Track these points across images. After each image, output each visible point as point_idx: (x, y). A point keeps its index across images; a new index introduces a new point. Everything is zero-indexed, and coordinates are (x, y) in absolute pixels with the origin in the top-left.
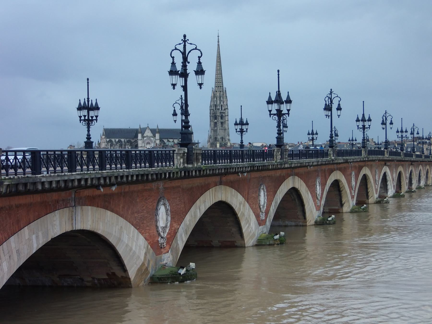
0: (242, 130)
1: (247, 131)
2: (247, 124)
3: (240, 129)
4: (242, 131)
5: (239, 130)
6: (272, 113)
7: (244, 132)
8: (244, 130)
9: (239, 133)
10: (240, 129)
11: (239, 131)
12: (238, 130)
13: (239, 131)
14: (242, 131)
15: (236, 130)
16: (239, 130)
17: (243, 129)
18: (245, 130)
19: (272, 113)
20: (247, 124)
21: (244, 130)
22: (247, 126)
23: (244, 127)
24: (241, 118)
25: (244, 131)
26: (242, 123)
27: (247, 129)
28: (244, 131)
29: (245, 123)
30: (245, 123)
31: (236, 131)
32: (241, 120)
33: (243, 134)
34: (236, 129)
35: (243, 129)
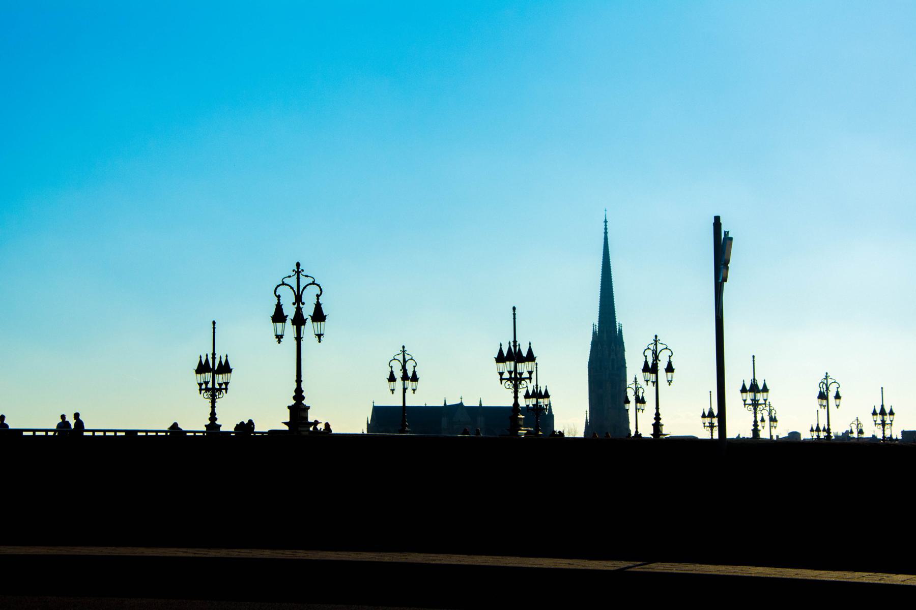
7: (523, 382)
8: (523, 376)
9: (509, 382)
10: (510, 372)
17: (521, 374)
18: (526, 375)
20: (531, 357)
21: (523, 376)
24: (515, 342)
25: (524, 379)
28: (524, 379)
29: (525, 354)
30: (525, 354)
31: (502, 379)
32: (515, 346)
35: (521, 374)
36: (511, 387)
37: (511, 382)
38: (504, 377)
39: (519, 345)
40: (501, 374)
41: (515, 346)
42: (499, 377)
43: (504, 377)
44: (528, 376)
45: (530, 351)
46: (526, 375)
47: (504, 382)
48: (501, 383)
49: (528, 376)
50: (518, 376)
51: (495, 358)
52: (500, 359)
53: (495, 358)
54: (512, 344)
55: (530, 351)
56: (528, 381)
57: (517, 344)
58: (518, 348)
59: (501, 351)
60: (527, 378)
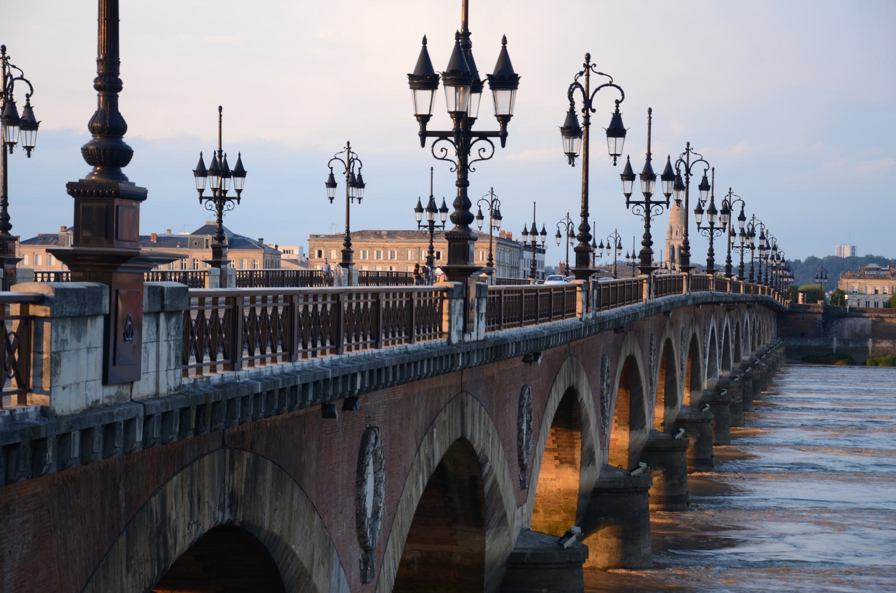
0: (220, 193)
1: (239, 199)
2: (240, 172)
3: (215, 190)
4: (220, 198)
5: (211, 194)
7: (227, 203)
8: (228, 195)
9: (212, 202)
10: (215, 190)
11: (210, 199)
12: (208, 193)
13: (210, 199)
14: (220, 198)
15: (201, 194)
16: (211, 194)
17: (225, 192)
18: (231, 193)
20: (240, 172)
21: (228, 195)
22: (239, 179)
23: (230, 185)
24: (220, 151)
25: (230, 199)
26: (220, 169)
28: (230, 199)
29: (232, 167)
30: (232, 167)
31: (201, 198)
32: (220, 156)
33: (225, 207)
34: (201, 191)
35: (225, 192)
37: (215, 202)
38: (204, 195)
39: (225, 155)
41: (220, 156)
43: (204, 195)
44: (235, 195)
45: (240, 164)
47: (204, 201)
48: (201, 203)
49: (235, 195)
50: (223, 195)
51: (194, 171)
52: (201, 171)
53: (194, 171)
54: (217, 153)
55: (240, 164)
57: (223, 154)
58: (223, 158)
59: (201, 163)
60: (234, 198)
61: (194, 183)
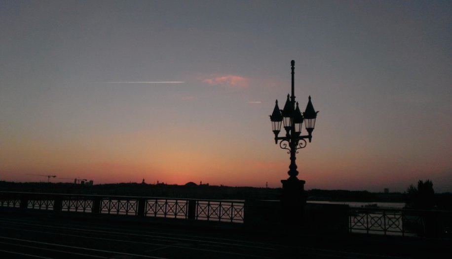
1: (310, 137)
4: (293, 139)
6: (279, 136)
7: (301, 141)
8: (301, 135)
9: (286, 142)
11: (283, 139)
13: (283, 139)
14: (293, 139)
17: (299, 133)
18: (304, 133)
19: (279, 136)
21: (301, 135)
24: (293, 97)
25: (302, 138)
27: (310, 130)
28: (302, 138)
29: (303, 109)
30: (303, 109)
31: (277, 139)
36: (288, 147)
40: (276, 132)
42: (274, 136)
44: (307, 134)
45: (310, 106)
46: (304, 133)
47: (279, 141)
48: (276, 143)
49: (307, 134)
52: (276, 116)
55: (310, 106)
56: (307, 140)
61: (269, 125)
